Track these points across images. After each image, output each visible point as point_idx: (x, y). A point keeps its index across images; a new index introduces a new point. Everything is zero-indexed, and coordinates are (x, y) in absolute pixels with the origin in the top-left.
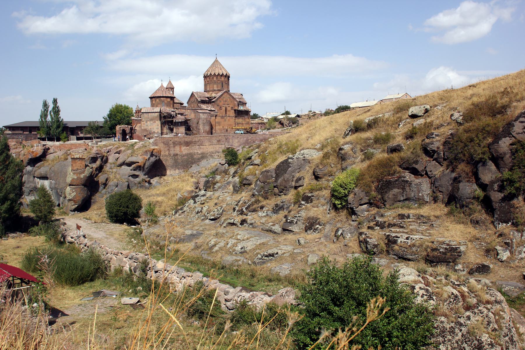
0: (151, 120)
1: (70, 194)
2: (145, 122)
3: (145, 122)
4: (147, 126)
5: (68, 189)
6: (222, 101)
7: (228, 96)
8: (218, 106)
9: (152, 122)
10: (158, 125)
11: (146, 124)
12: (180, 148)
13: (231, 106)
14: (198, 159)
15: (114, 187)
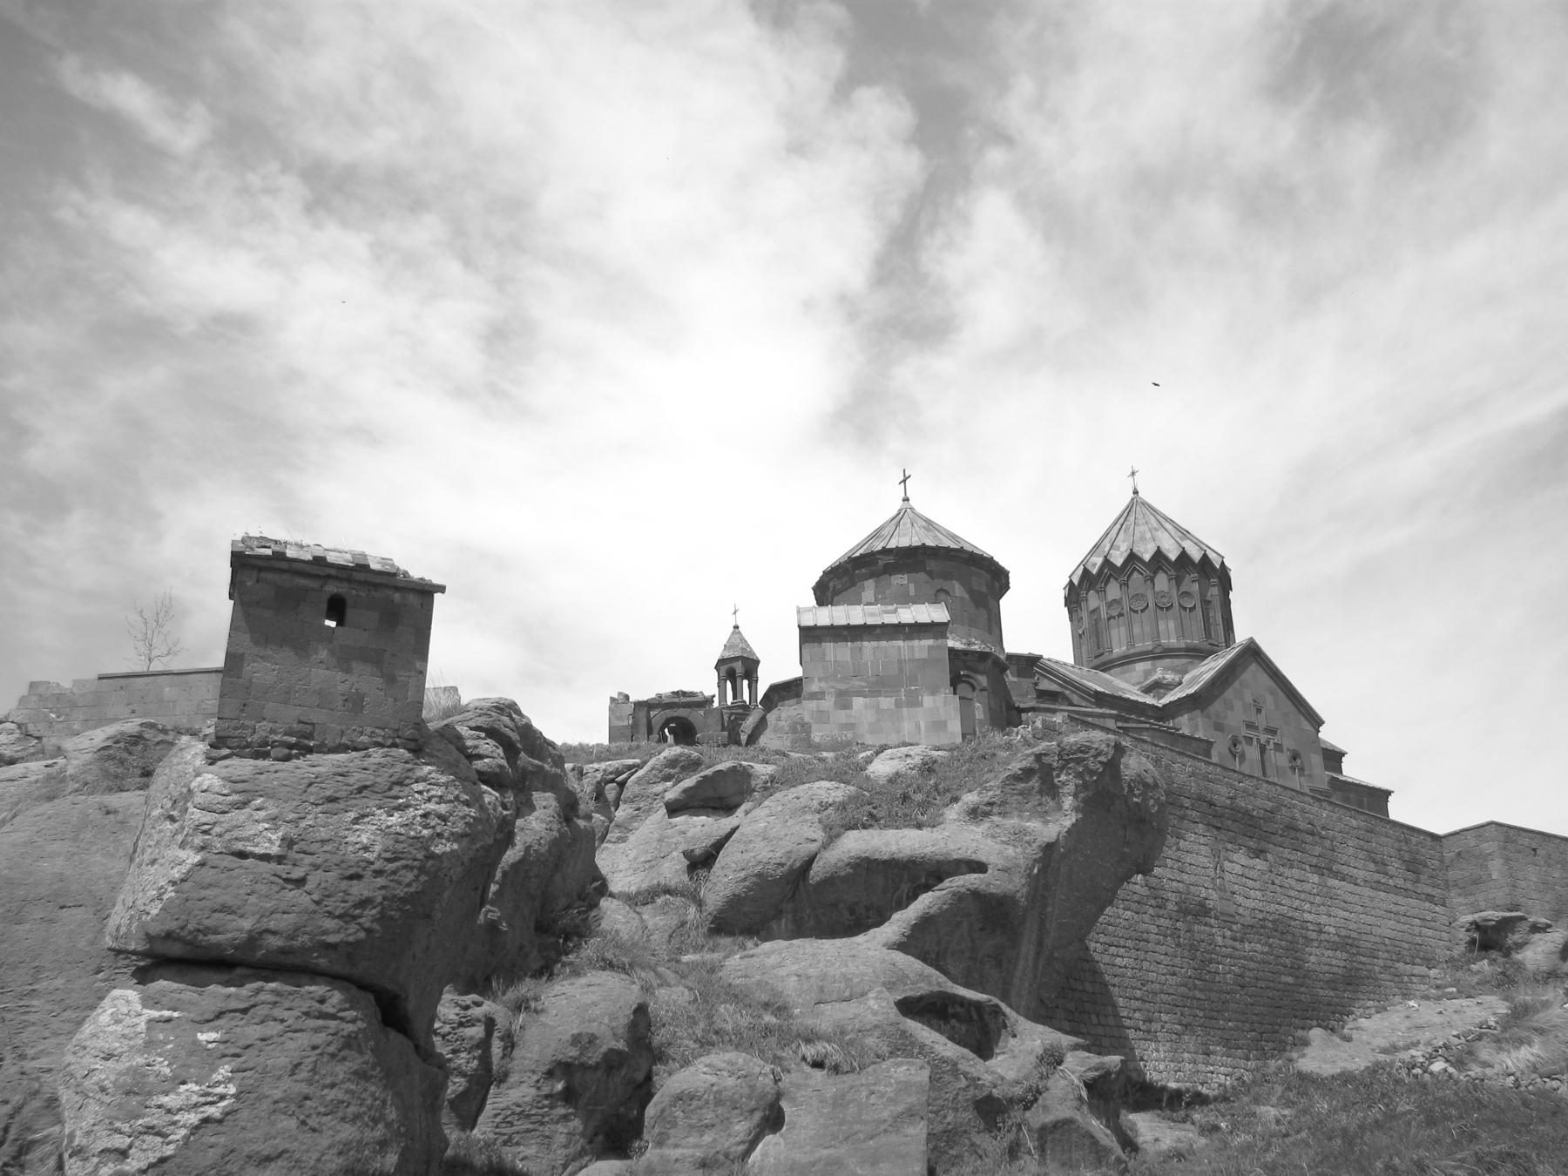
0: (880, 686)
1: (137, 1088)
2: (828, 704)
3: (828, 704)
4: (850, 726)
5: (125, 1010)
6: (1238, 704)
7: (1265, 679)
8: (1219, 727)
9: (886, 702)
10: (939, 726)
11: (841, 716)
12: (1216, 854)
13: (1288, 744)
14: (1331, 984)
15: (741, 1128)
